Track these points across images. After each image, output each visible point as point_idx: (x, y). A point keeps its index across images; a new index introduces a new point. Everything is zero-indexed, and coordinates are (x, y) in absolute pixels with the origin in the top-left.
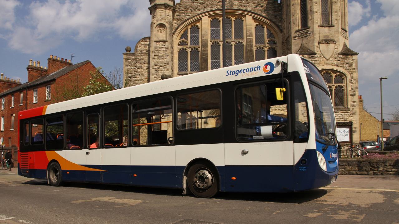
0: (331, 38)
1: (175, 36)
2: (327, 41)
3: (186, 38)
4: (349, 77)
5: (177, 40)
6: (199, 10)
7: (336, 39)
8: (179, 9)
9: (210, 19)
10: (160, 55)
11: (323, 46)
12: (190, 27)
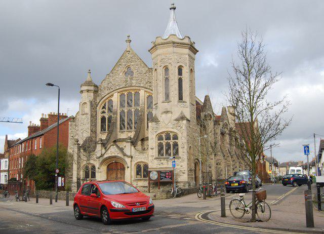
0: (169, 110)
2: (167, 112)
9: (119, 94)
11: (164, 115)
12: (107, 101)
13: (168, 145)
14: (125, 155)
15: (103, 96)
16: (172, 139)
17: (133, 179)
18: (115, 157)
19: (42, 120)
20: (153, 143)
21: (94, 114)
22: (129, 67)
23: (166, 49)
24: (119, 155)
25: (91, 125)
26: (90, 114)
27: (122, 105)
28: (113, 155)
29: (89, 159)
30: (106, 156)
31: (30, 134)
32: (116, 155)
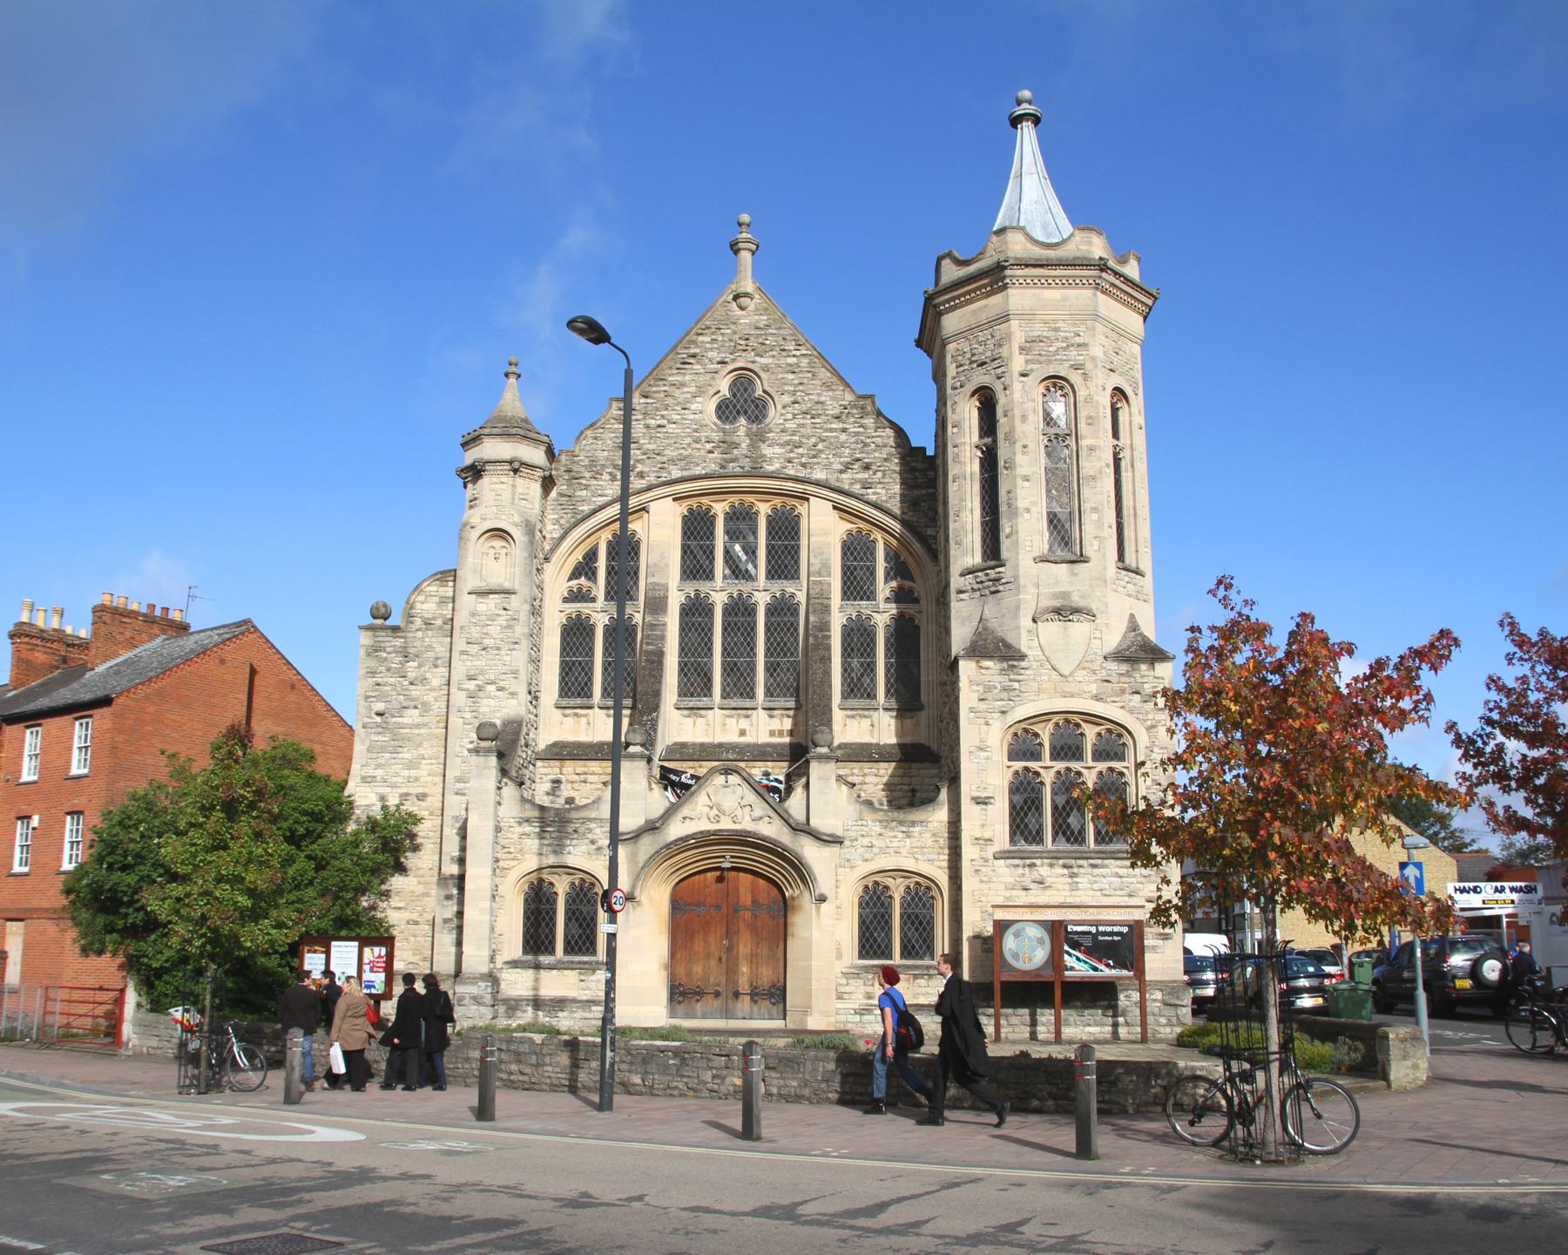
0: (1077, 601)
1: (549, 569)
2: (1065, 612)
5: (557, 580)
7: (1094, 607)
8: (569, 471)
9: (681, 509)
10: (487, 642)
11: (1051, 630)
12: (605, 536)
15: (586, 508)
28: (726, 824)
29: (559, 849)
30: (676, 829)
32: (746, 825)
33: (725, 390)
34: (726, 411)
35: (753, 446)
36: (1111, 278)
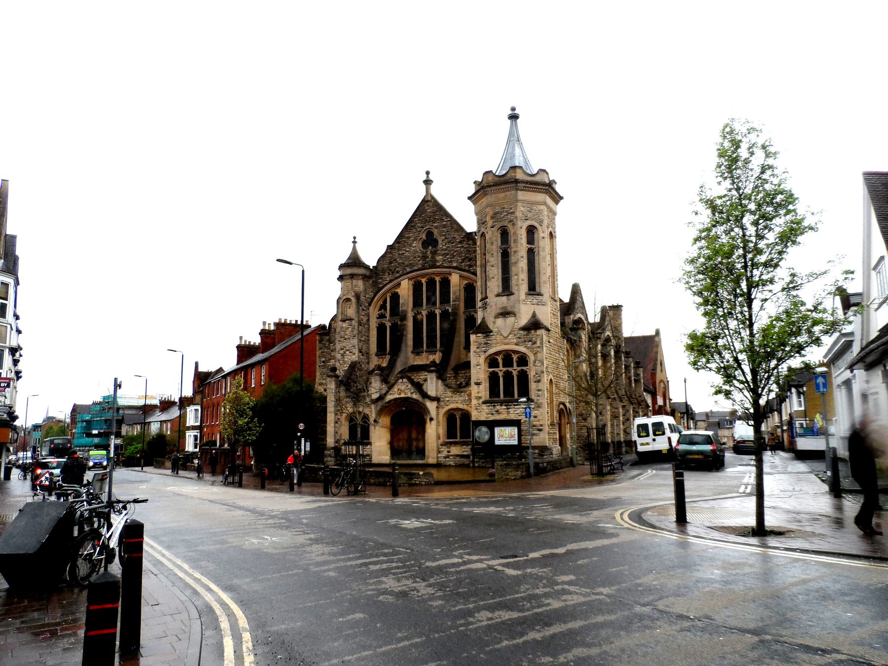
0: (509, 309)
1: (371, 308)
2: (505, 313)
3: (386, 310)
4: (531, 358)
5: (374, 312)
6: (398, 272)
7: (516, 310)
9: (411, 282)
11: (500, 321)
12: (389, 295)
13: (508, 376)
14: (425, 395)
16: (515, 364)
17: (441, 441)
18: (407, 399)
19: (263, 333)
20: (479, 371)
21: (365, 319)
22: (430, 234)
23: (503, 195)
24: (415, 396)
25: (360, 341)
26: (356, 319)
27: (417, 303)
28: (403, 395)
30: (389, 397)
31: (240, 359)
32: (409, 395)
33: (424, 237)
34: (425, 244)
35: (433, 257)
36: (523, 185)
